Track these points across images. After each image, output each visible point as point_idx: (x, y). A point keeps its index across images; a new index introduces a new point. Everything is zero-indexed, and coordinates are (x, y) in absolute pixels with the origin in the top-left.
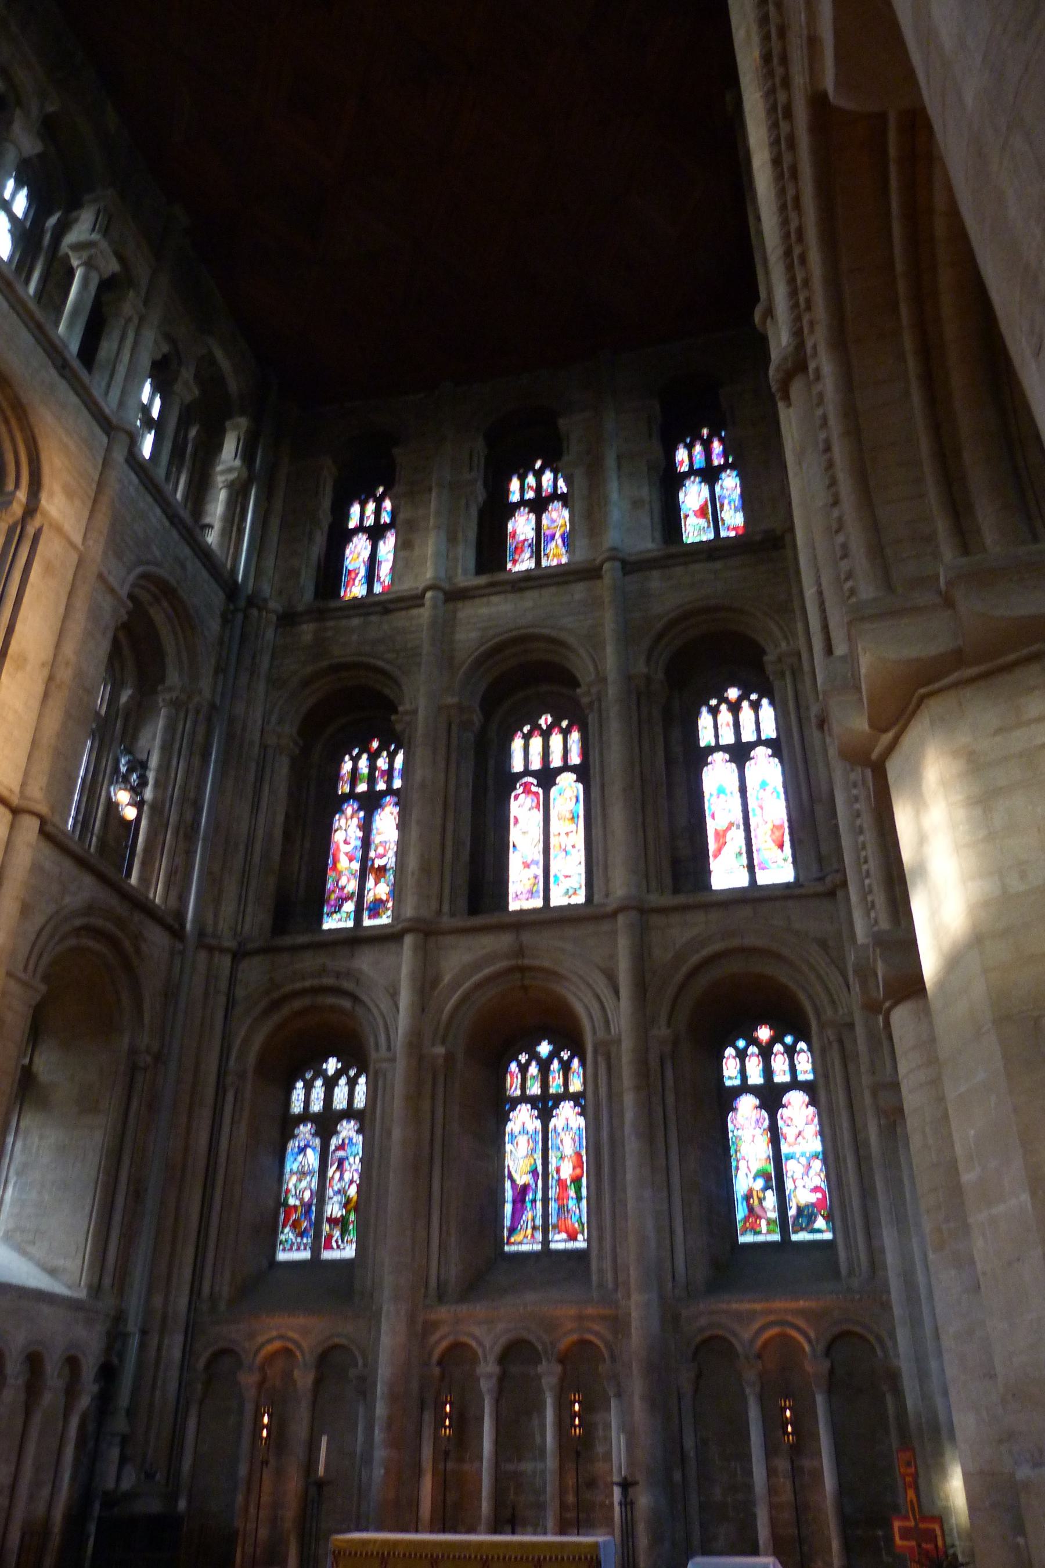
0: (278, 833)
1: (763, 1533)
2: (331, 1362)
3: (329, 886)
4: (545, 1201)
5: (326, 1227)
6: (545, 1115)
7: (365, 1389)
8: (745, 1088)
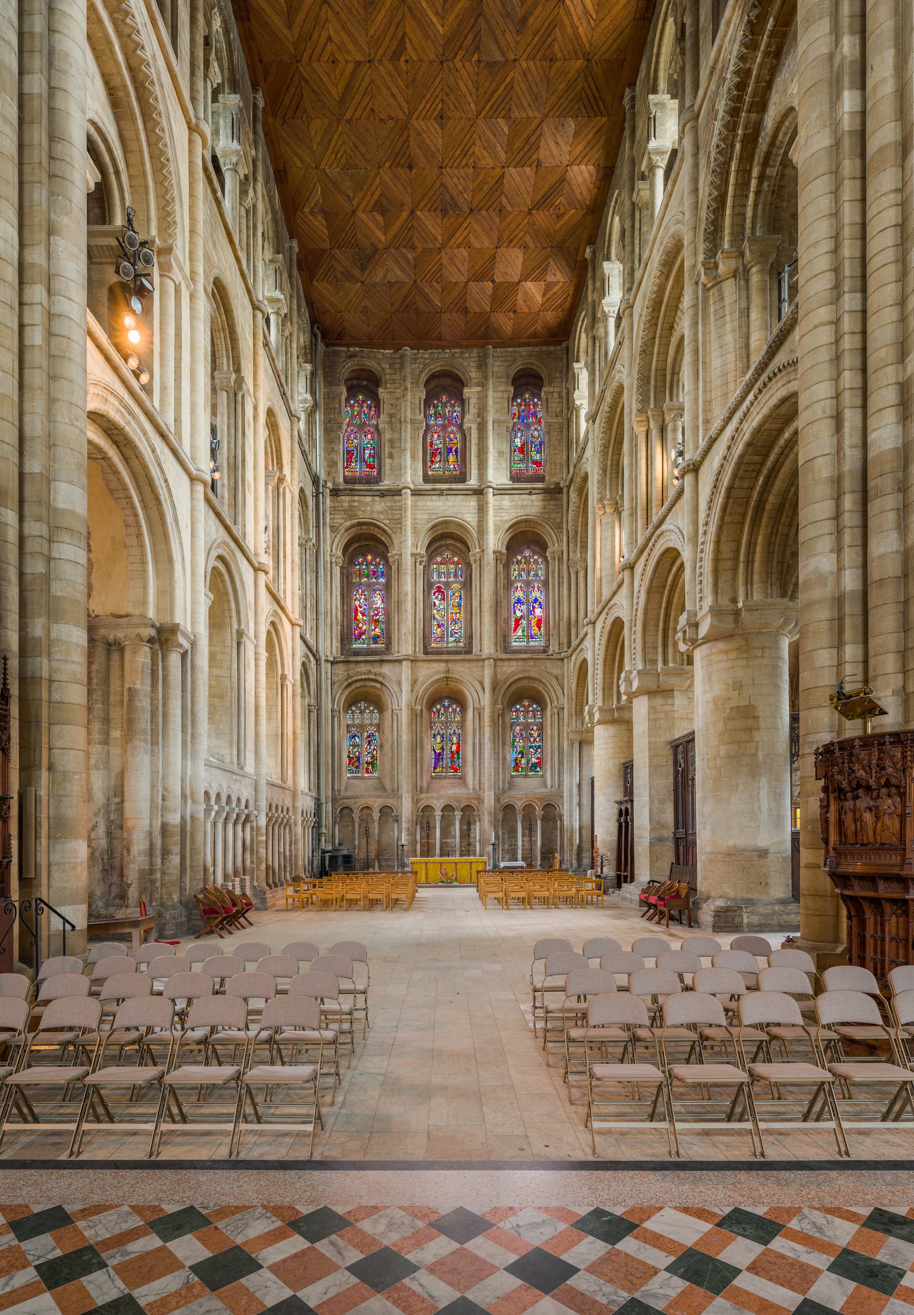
1: (520, 856)
2: (385, 811)
7: (397, 820)
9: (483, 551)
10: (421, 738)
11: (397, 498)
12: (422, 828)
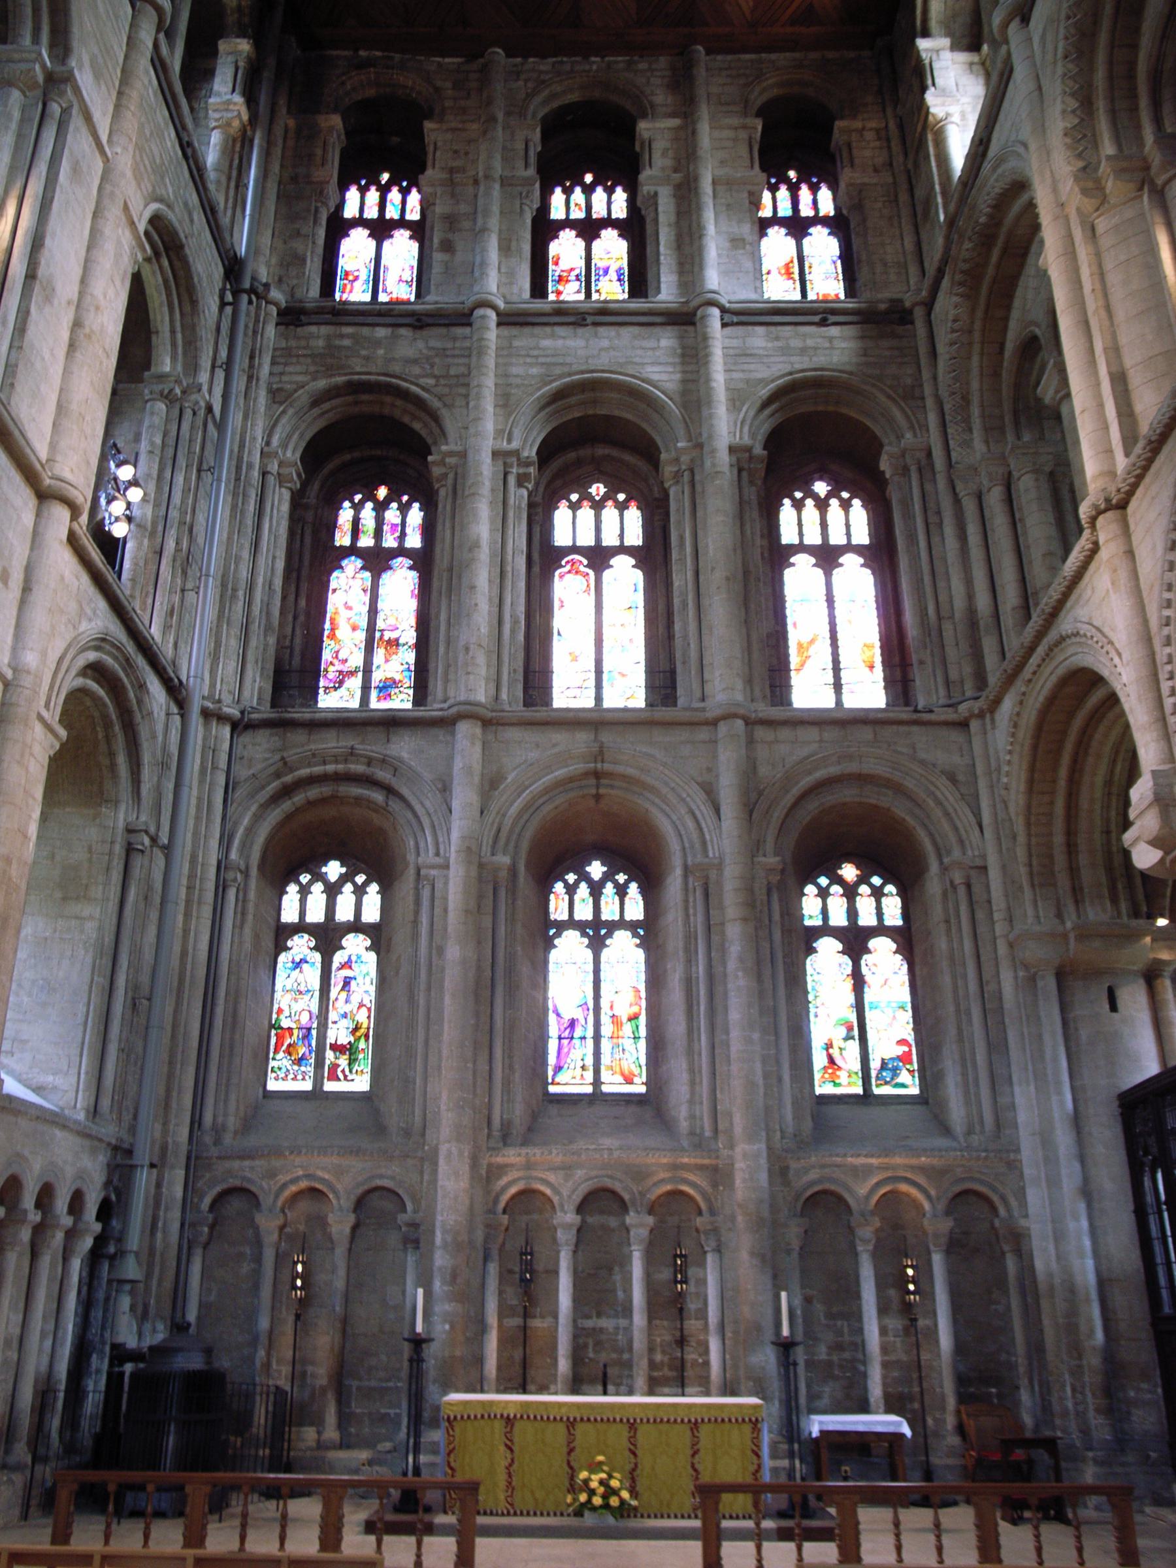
0: (278, 582)
1: (876, 1390)
2: (375, 1206)
3: (327, 655)
4: (597, 1037)
5: (330, 1055)
6: (597, 945)
7: (416, 1238)
8: (825, 930)
9: (700, 446)
10: (511, 958)
11: (459, 331)
12: (505, 1275)
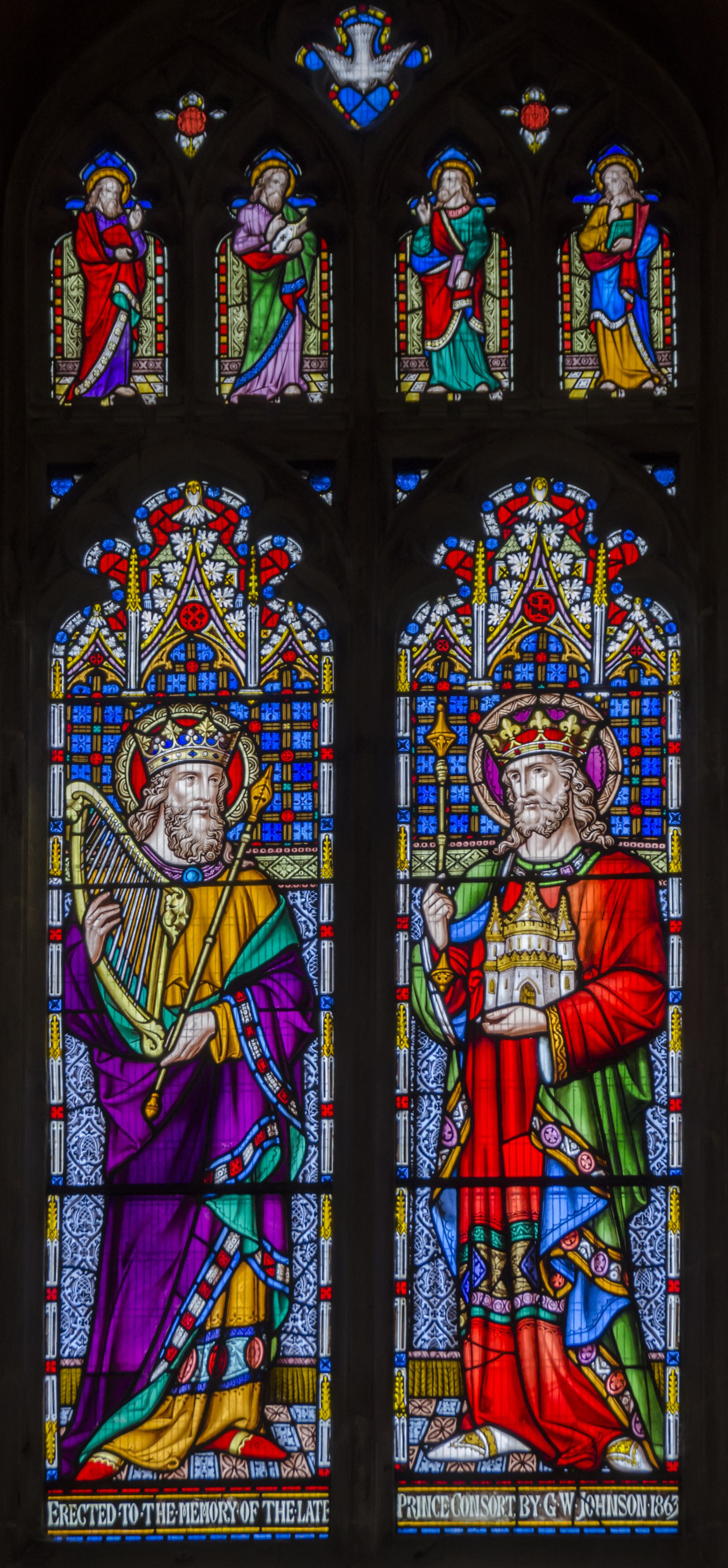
4: (365, 1186)
